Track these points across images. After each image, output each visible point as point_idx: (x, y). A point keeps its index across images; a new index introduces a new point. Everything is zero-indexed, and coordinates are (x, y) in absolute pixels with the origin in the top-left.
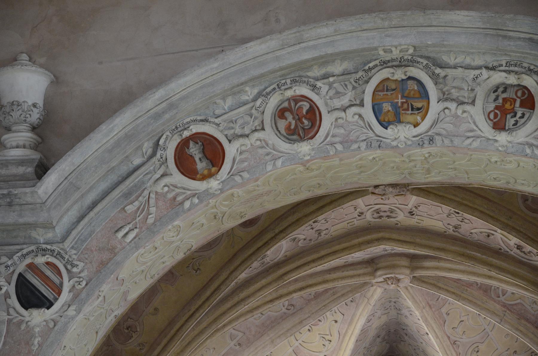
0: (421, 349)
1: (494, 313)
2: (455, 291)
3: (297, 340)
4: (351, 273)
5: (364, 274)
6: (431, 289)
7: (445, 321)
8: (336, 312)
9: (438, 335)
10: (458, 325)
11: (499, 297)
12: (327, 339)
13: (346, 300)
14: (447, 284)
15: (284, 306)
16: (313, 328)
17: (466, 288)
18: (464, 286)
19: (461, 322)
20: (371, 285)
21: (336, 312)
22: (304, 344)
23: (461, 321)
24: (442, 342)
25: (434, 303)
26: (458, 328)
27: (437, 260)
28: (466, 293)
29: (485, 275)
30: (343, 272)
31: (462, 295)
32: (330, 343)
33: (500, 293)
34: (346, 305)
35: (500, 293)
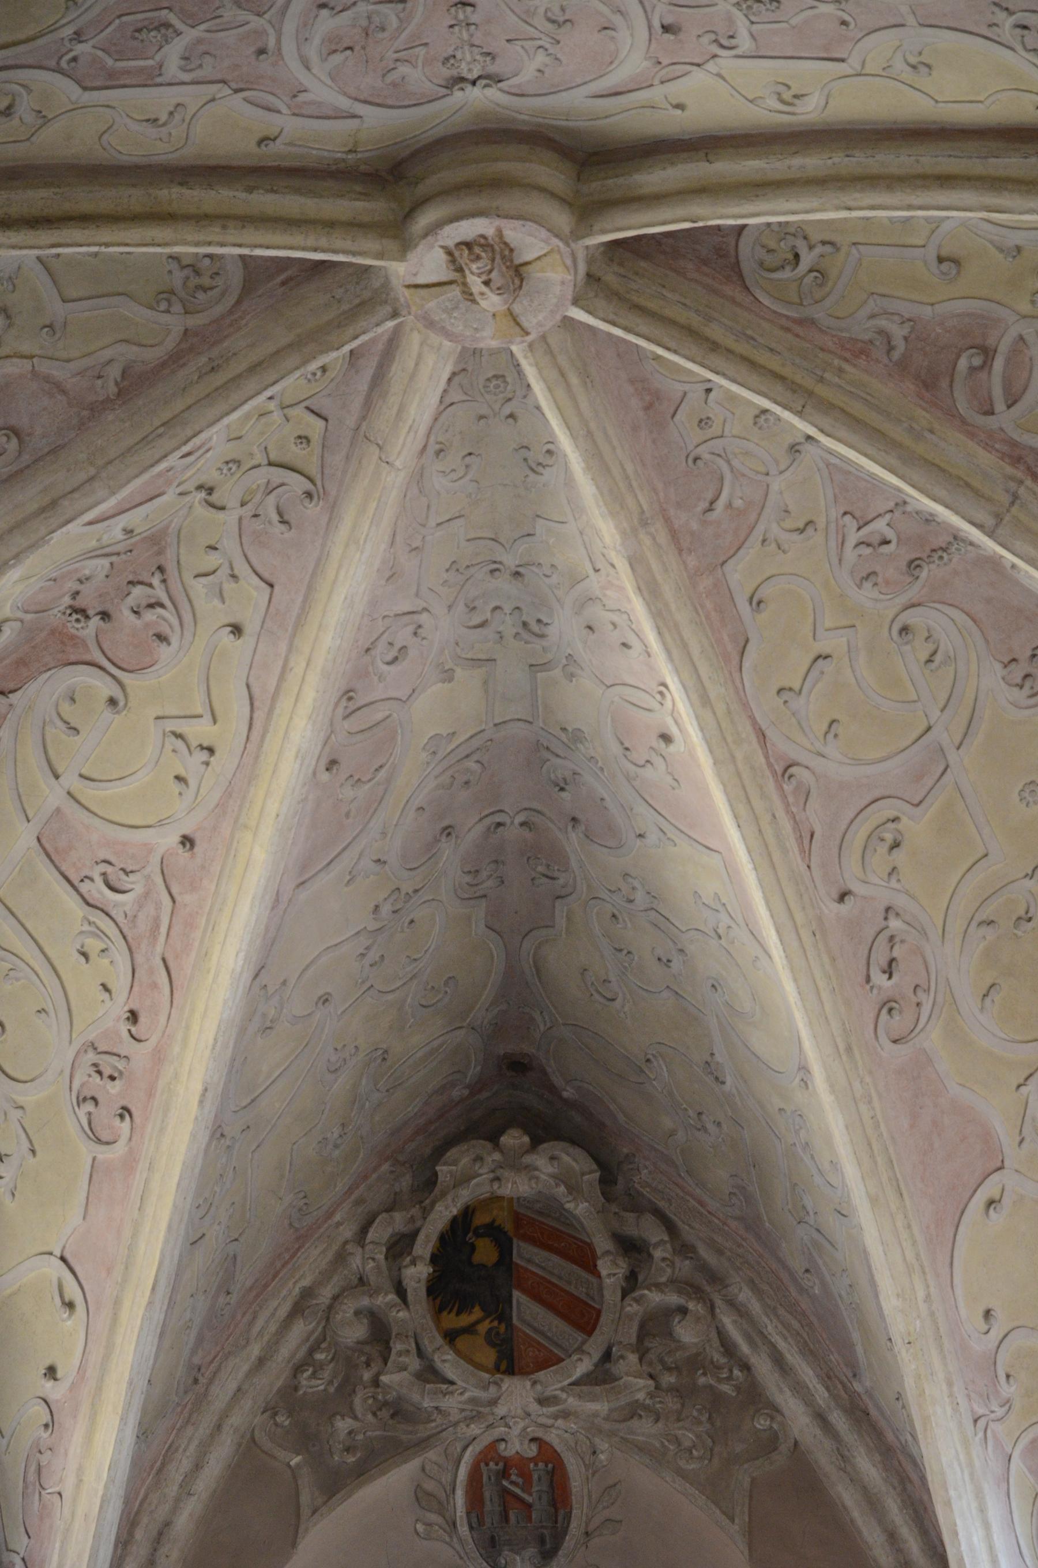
0: (639, 896)
1: (968, 485)
2: (787, 371)
3: (57, 777)
4: (292, 204)
5: (356, 226)
6: (672, 344)
7: (747, 641)
8: (233, 576)
9: (712, 695)
10: (805, 680)
11: (991, 412)
12: (194, 743)
13: (265, 389)
14: (749, 332)
16: (129, 690)
17: (836, 362)
18: (830, 352)
19: (820, 661)
20: (388, 309)
21: (233, 576)
22: (88, 793)
23: (819, 657)
24: (729, 739)
25: (695, 526)
27: (702, 154)
28: (836, 380)
29: (924, 177)
30: (250, 190)
31: (821, 390)
32: (207, 764)
33: (997, 392)
34: (283, 522)
35: (997, 392)
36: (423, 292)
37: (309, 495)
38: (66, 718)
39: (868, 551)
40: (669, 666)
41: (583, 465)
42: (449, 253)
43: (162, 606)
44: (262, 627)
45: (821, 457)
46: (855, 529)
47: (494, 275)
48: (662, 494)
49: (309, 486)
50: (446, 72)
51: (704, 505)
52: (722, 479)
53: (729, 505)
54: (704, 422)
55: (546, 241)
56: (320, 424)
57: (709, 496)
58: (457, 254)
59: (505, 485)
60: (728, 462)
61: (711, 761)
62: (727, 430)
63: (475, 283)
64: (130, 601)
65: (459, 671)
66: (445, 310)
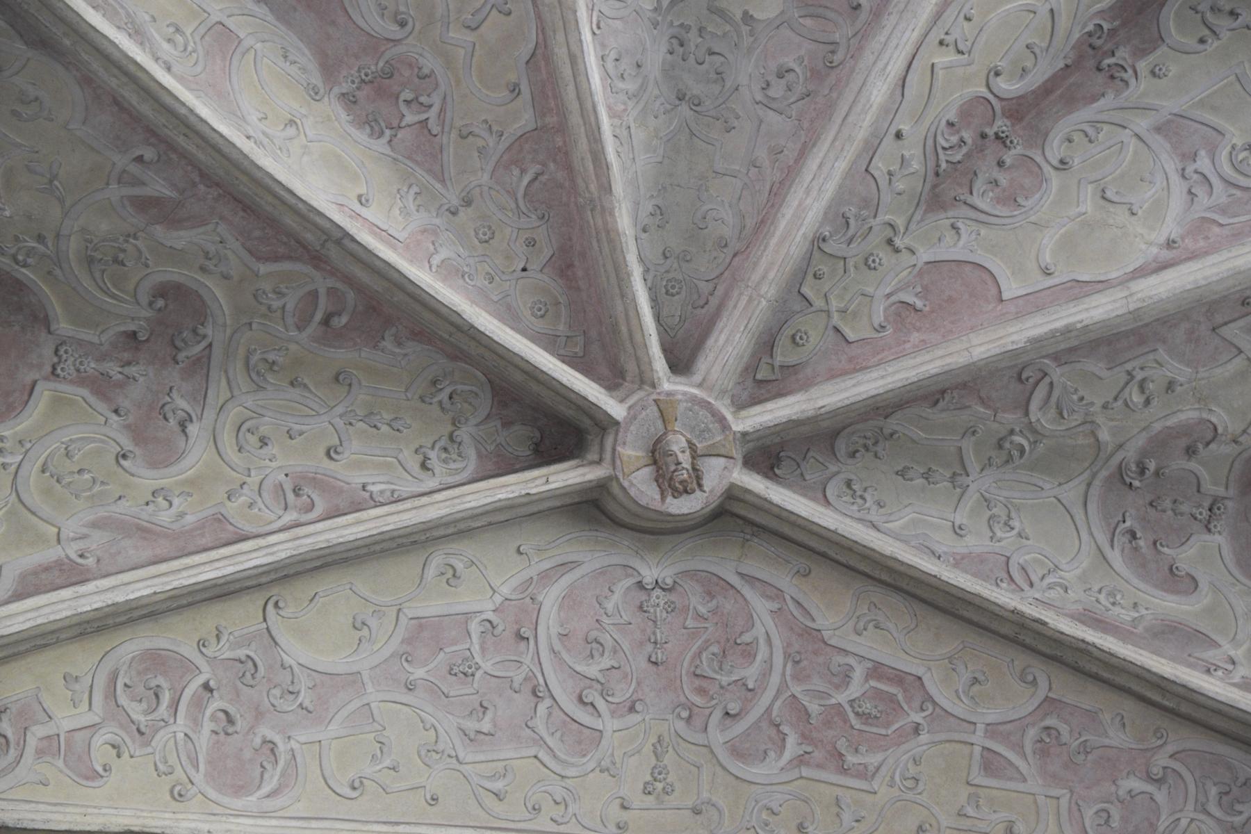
7: (527, 62)
15: (1051, 384)
20: (748, 438)
25: (552, 166)
26: (489, 7)
33: (323, 301)
36: (723, 451)
37: (824, 240)
38: (1032, 55)
39: (423, 99)
40: (596, 99)
41: (632, 279)
42: (700, 486)
43: (944, 149)
44: (882, 140)
45: (448, 190)
46: (430, 121)
47: (673, 468)
48: (573, 200)
49: (823, 246)
50: (673, 597)
51: (543, 178)
52: (525, 195)
53: (523, 171)
54: (531, 243)
55: (632, 484)
56: (805, 290)
57: (537, 183)
58: (695, 485)
59: (679, 186)
60: (518, 206)
61: (578, 14)
62: (515, 235)
63: (685, 459)
64: (965, 150)
65: (738, 16)
66: (709, 430)
